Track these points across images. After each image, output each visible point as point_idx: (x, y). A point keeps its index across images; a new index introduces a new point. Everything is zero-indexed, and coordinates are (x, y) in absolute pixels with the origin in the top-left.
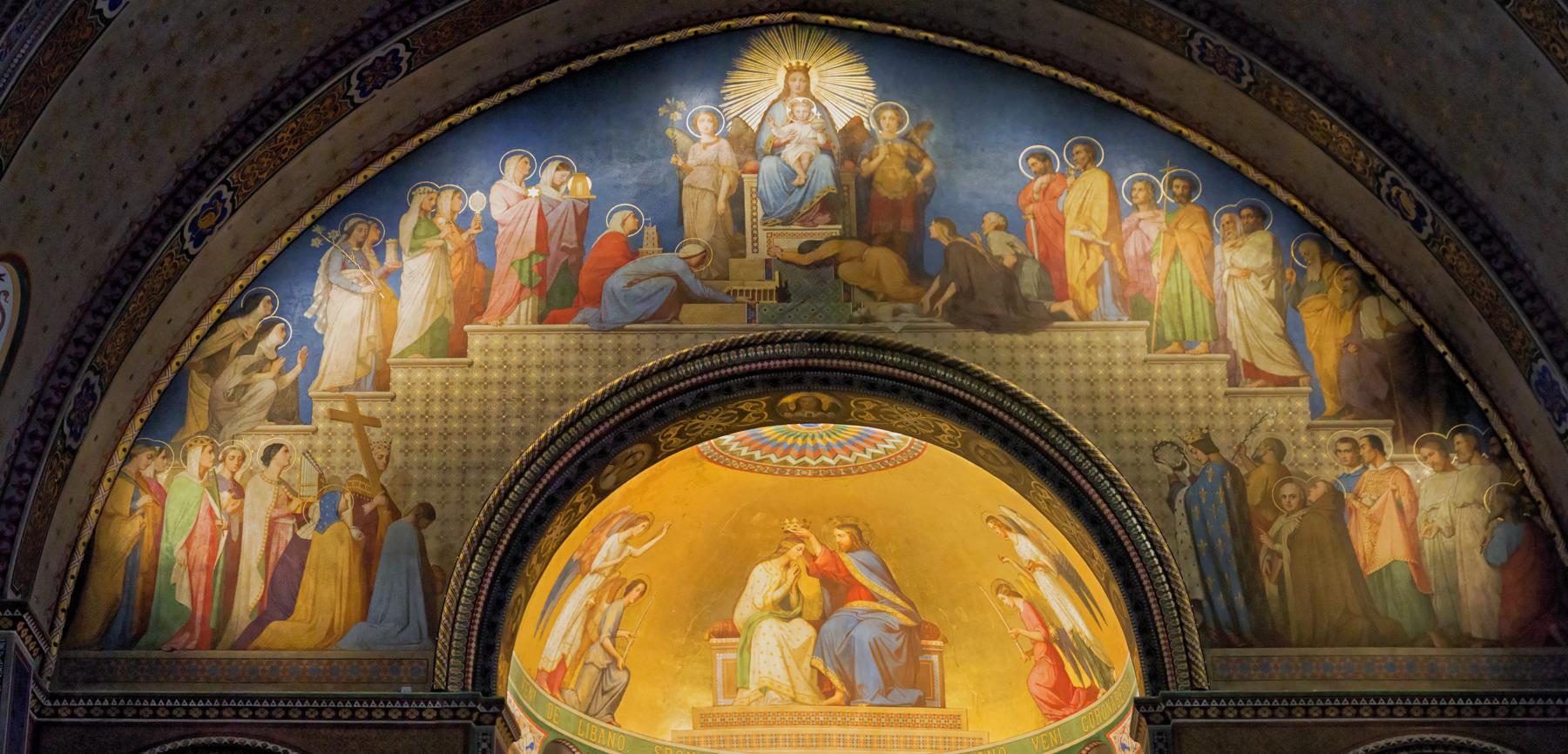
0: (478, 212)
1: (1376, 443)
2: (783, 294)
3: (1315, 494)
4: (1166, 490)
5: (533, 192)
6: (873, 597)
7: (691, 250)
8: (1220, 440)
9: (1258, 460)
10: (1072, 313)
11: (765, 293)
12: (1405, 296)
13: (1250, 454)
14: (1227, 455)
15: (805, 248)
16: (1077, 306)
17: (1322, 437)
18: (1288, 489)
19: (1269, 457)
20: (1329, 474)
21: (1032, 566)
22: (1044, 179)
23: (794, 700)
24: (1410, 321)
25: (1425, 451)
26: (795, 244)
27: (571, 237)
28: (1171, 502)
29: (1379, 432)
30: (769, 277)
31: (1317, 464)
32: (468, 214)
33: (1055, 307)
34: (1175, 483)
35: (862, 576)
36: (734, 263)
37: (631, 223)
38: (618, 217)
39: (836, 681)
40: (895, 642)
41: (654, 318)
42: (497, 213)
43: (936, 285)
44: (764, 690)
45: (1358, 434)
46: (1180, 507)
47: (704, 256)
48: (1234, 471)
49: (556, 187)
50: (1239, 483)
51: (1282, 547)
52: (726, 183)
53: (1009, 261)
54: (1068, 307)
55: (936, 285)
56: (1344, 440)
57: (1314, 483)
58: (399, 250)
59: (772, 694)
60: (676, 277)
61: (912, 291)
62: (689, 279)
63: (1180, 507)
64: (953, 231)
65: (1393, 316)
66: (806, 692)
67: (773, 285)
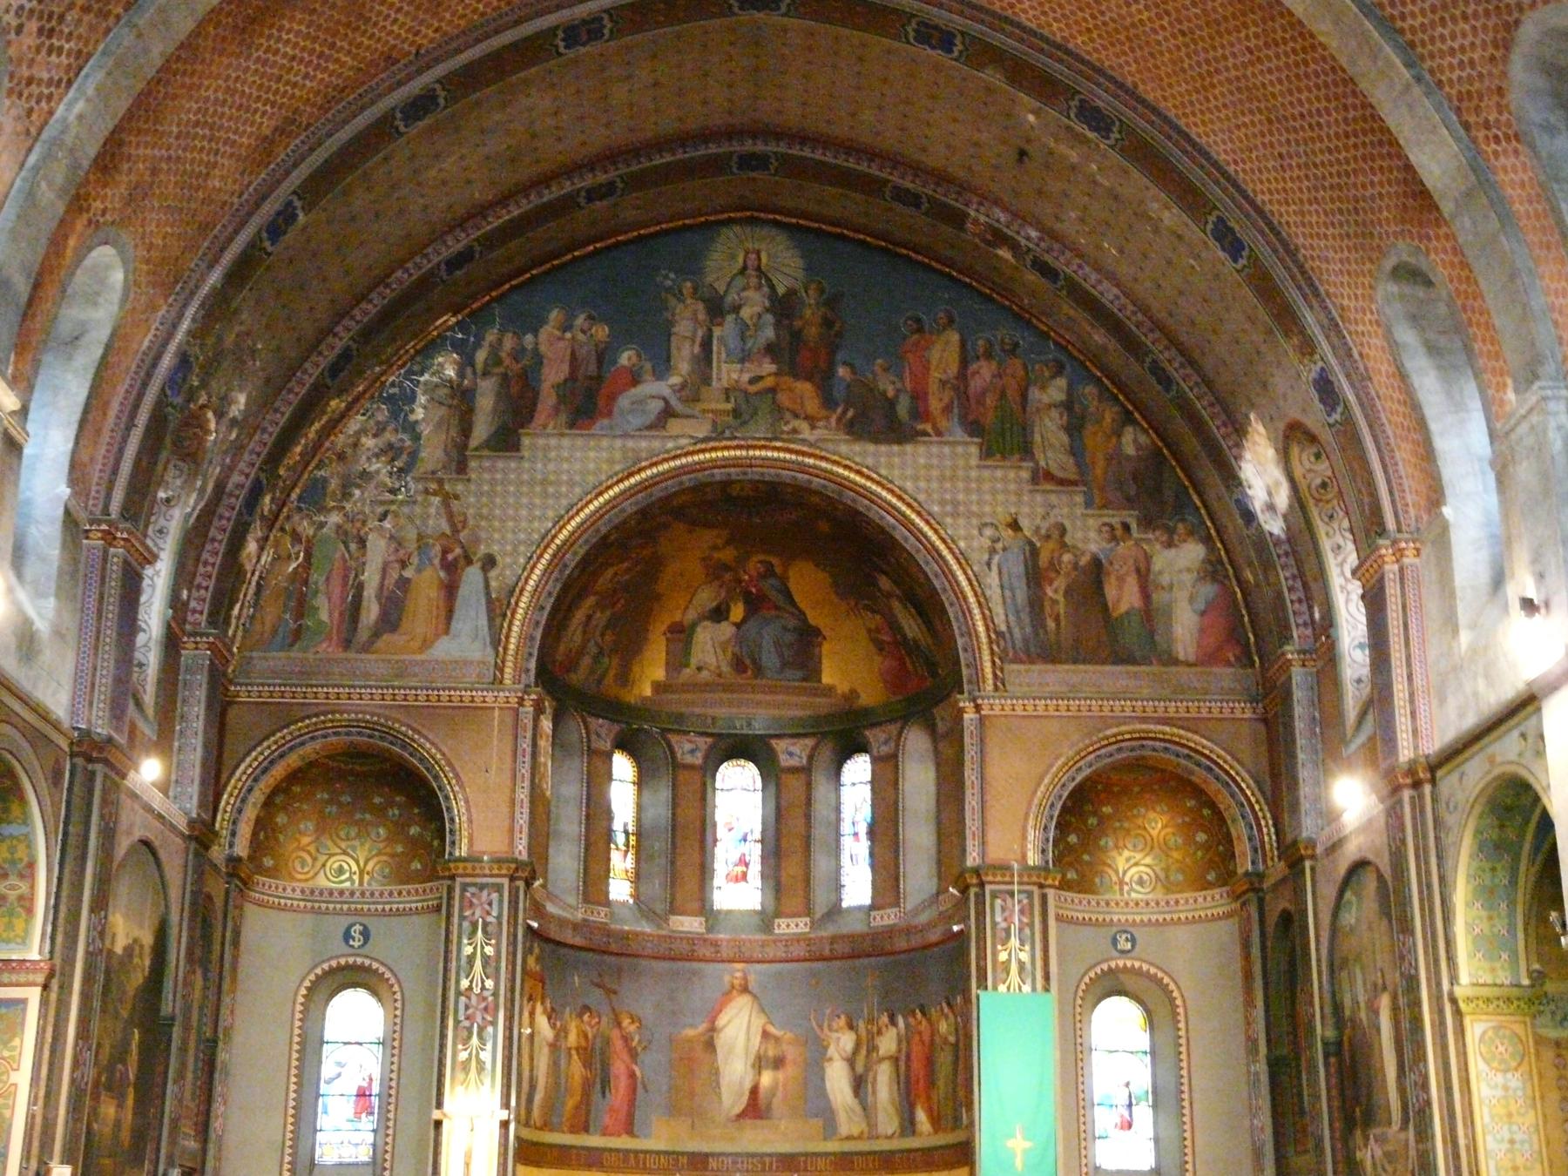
0: (530, 347)
1: (1126, 527)
2: (736, 413)
3: (1084, 561)
4: (986, 557)
5: (568, 335)
6: (777, 608)
7: (675, 380)
8: (1025, 523)
9: (1048, 537)
10: (930, 430)
11: (727, 413)
12: (1152, 427)
13: (1043, 532)
14: (1028, 533)
15: (754, 380)
16: (934, 427)
17: (1091, 522)
18: (1067, 557)
19: (1056, 535)
20: (1093, 547)
21: (889, 595)
22: (916, 336)
23: (720, 675)
24: (1153, 442)
25: (1158, 533)
26: (746, 377)
27: (592, 369)
28: (989, 564)
29: (1129, 520)
30: (728, 400)
31: (1086, 540)
32: (524, 349)
33: (920, 427)
34: (993, 551)
35: (773, 594)
36: (704, 389)
37: (634, 359)
38: (626, 355)
39: (748, 662)
40: (789, 638)
41: (650, 427)
42: (543, 348)
43: (839, 410)
44: (699, 669)
45: (1115, 521)
46: (994, 568)
47: (683, 386)
48: (1031, 543)
49: (583, 332)
50: (1035, 552)
51: (1060, 597)
52: (700, 333)
53: (890, 394)
54: (928, 428)
55: (839, 410)
56: (1105, 524)
57: (1083, 553)
58: (474, 373)
59: (705, 673)
60: (664, 399)
61: (824, 413)
62: (674, 402)
63: (994, 568)
64: (854, 372)
65: (1143, 439)
66: (725, 669)
67: (729, 406)
